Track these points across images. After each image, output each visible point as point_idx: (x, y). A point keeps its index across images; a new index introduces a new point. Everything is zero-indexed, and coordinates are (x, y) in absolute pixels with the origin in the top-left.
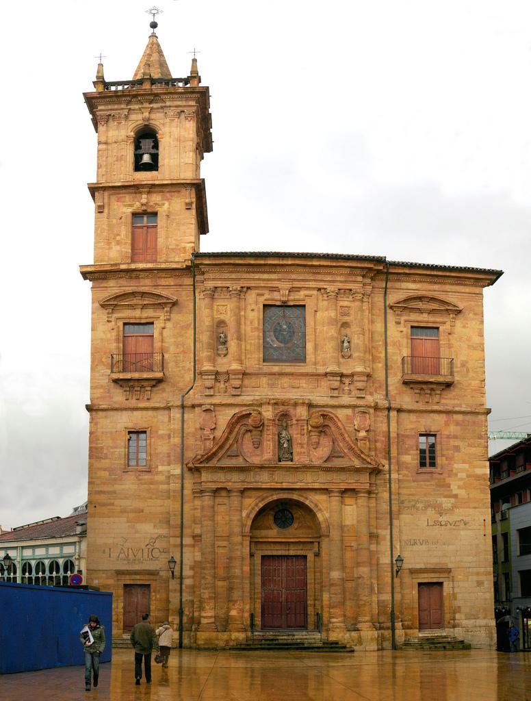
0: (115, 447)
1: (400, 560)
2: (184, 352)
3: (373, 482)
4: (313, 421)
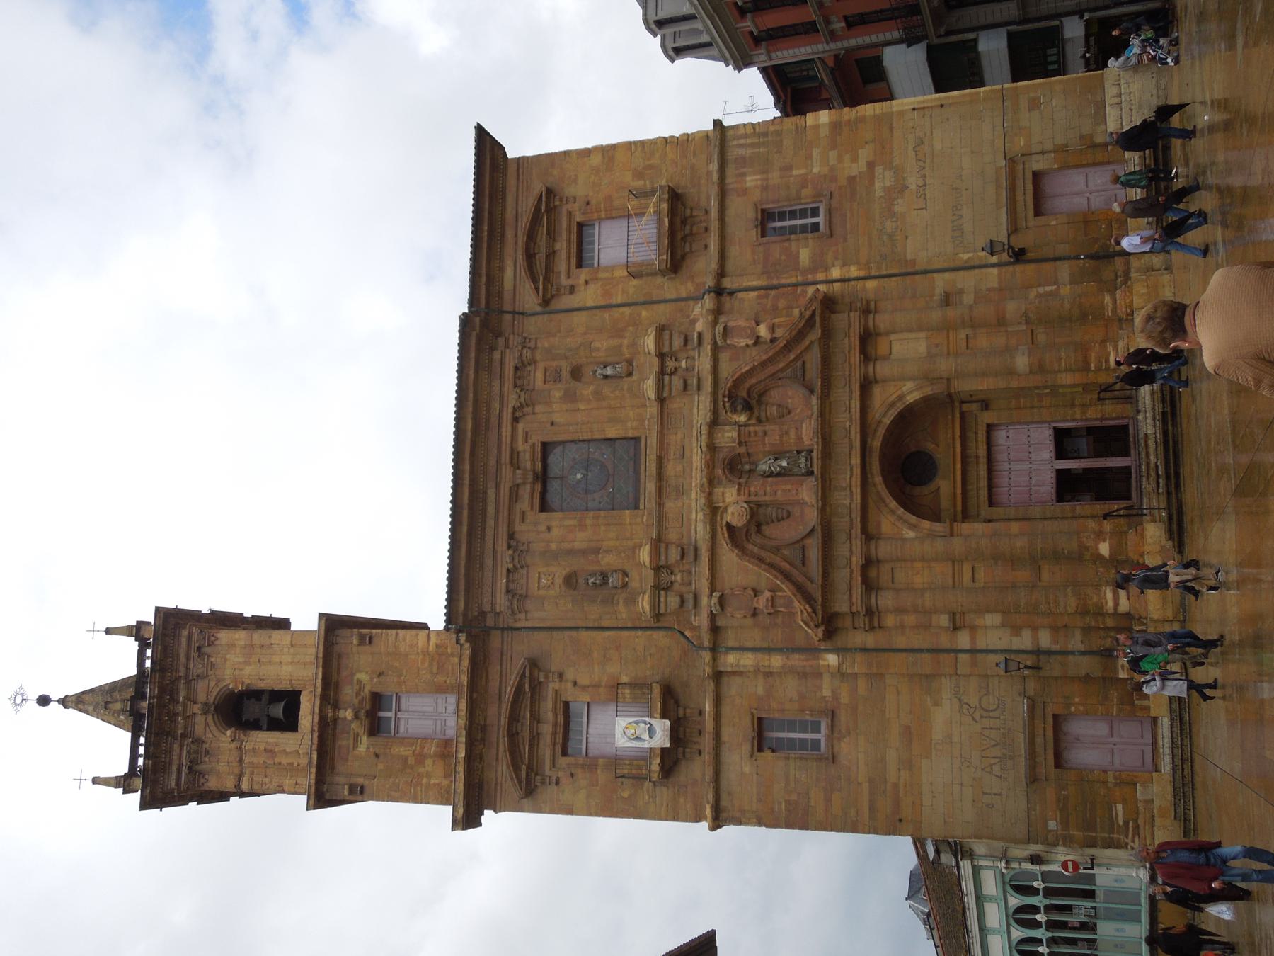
1: (992, 248)
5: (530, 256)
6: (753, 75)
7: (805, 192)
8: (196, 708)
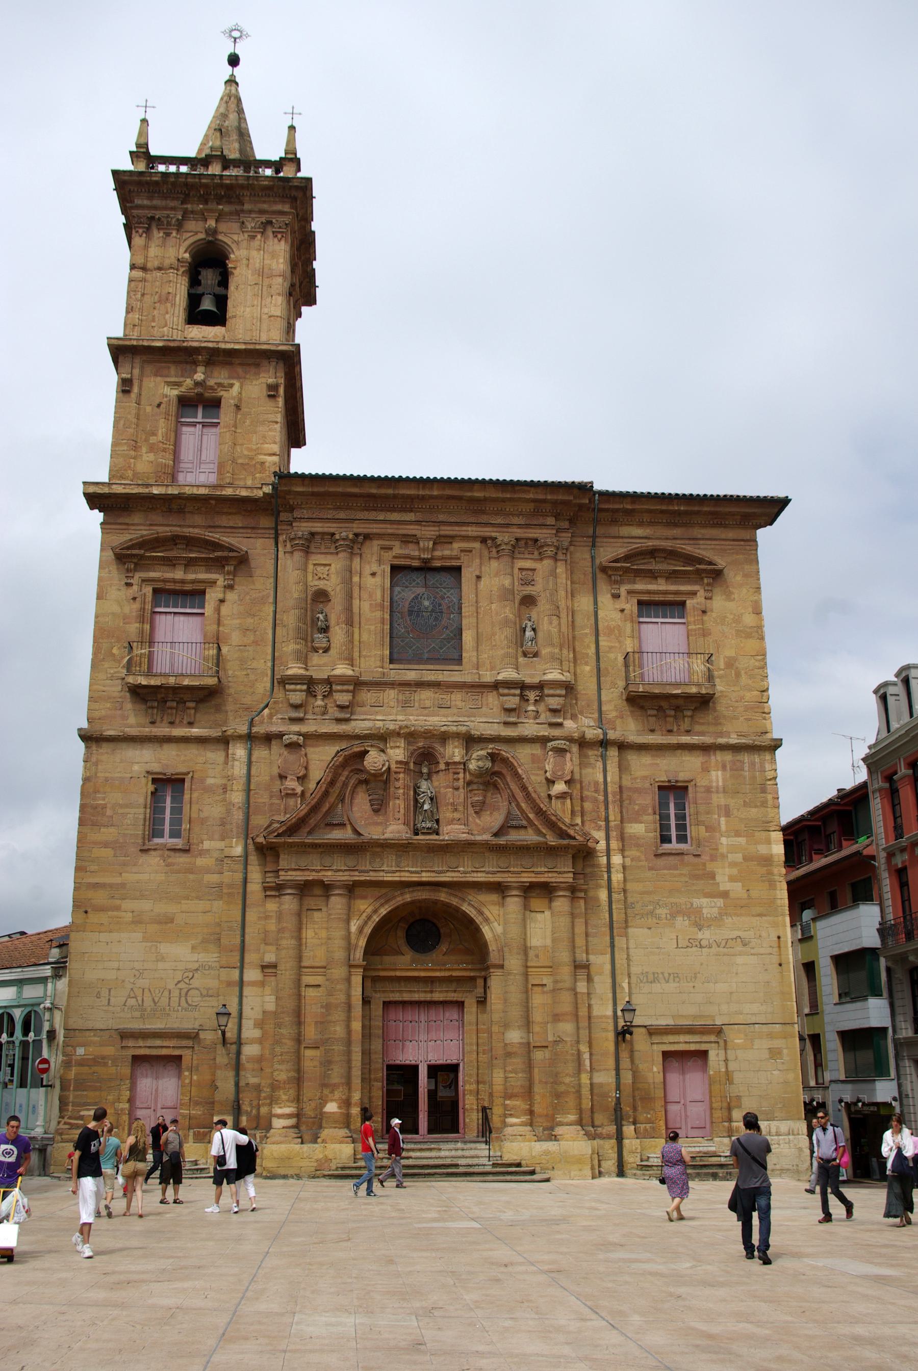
0: (127, 806)
1: (629, 1009)
2: (256, 643)
3: (579, 870)
4: (473, 766)
5: (653, 553)
6: (862, 775)
7: (702, 829)
8: (212, 223)
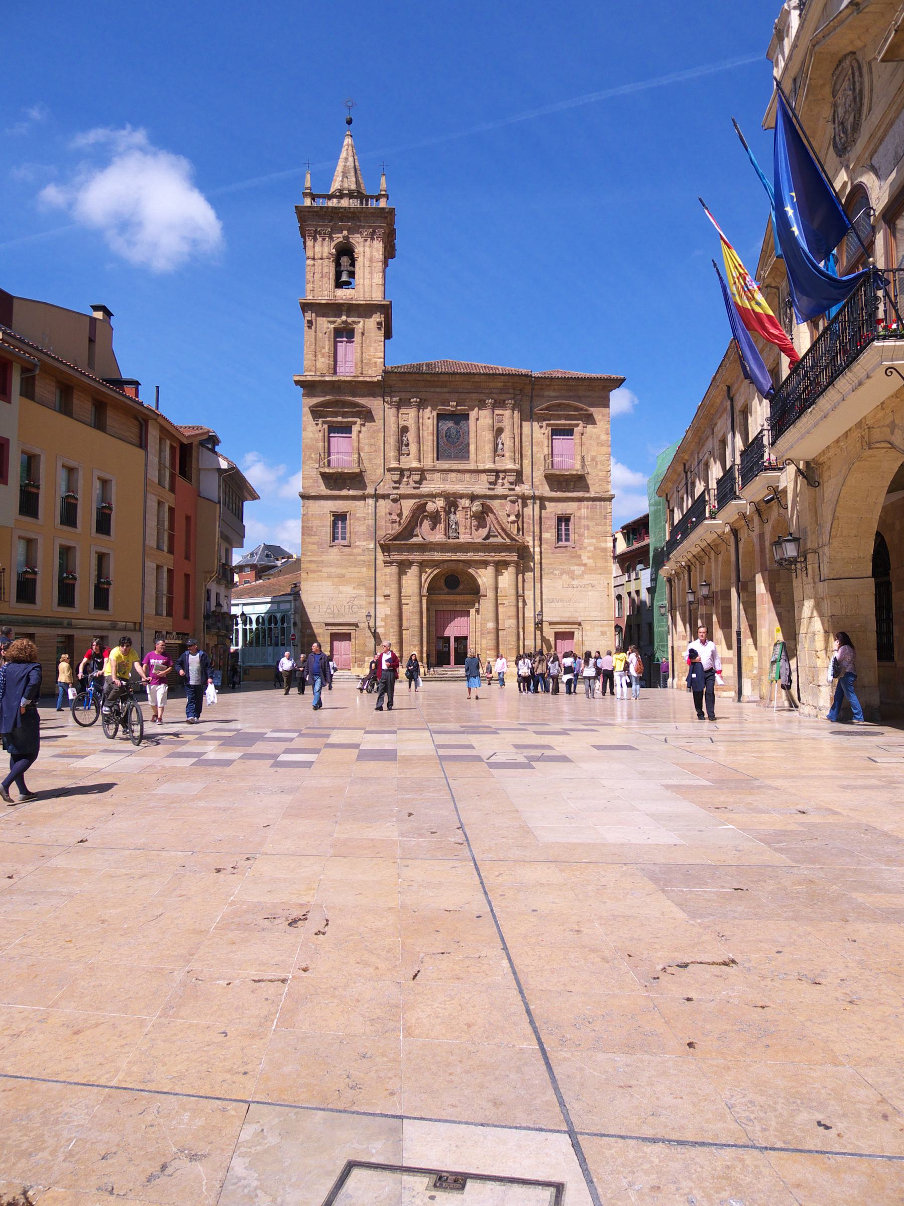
0: (322, 527)
4: (474, 509)
8: (345, 233)
